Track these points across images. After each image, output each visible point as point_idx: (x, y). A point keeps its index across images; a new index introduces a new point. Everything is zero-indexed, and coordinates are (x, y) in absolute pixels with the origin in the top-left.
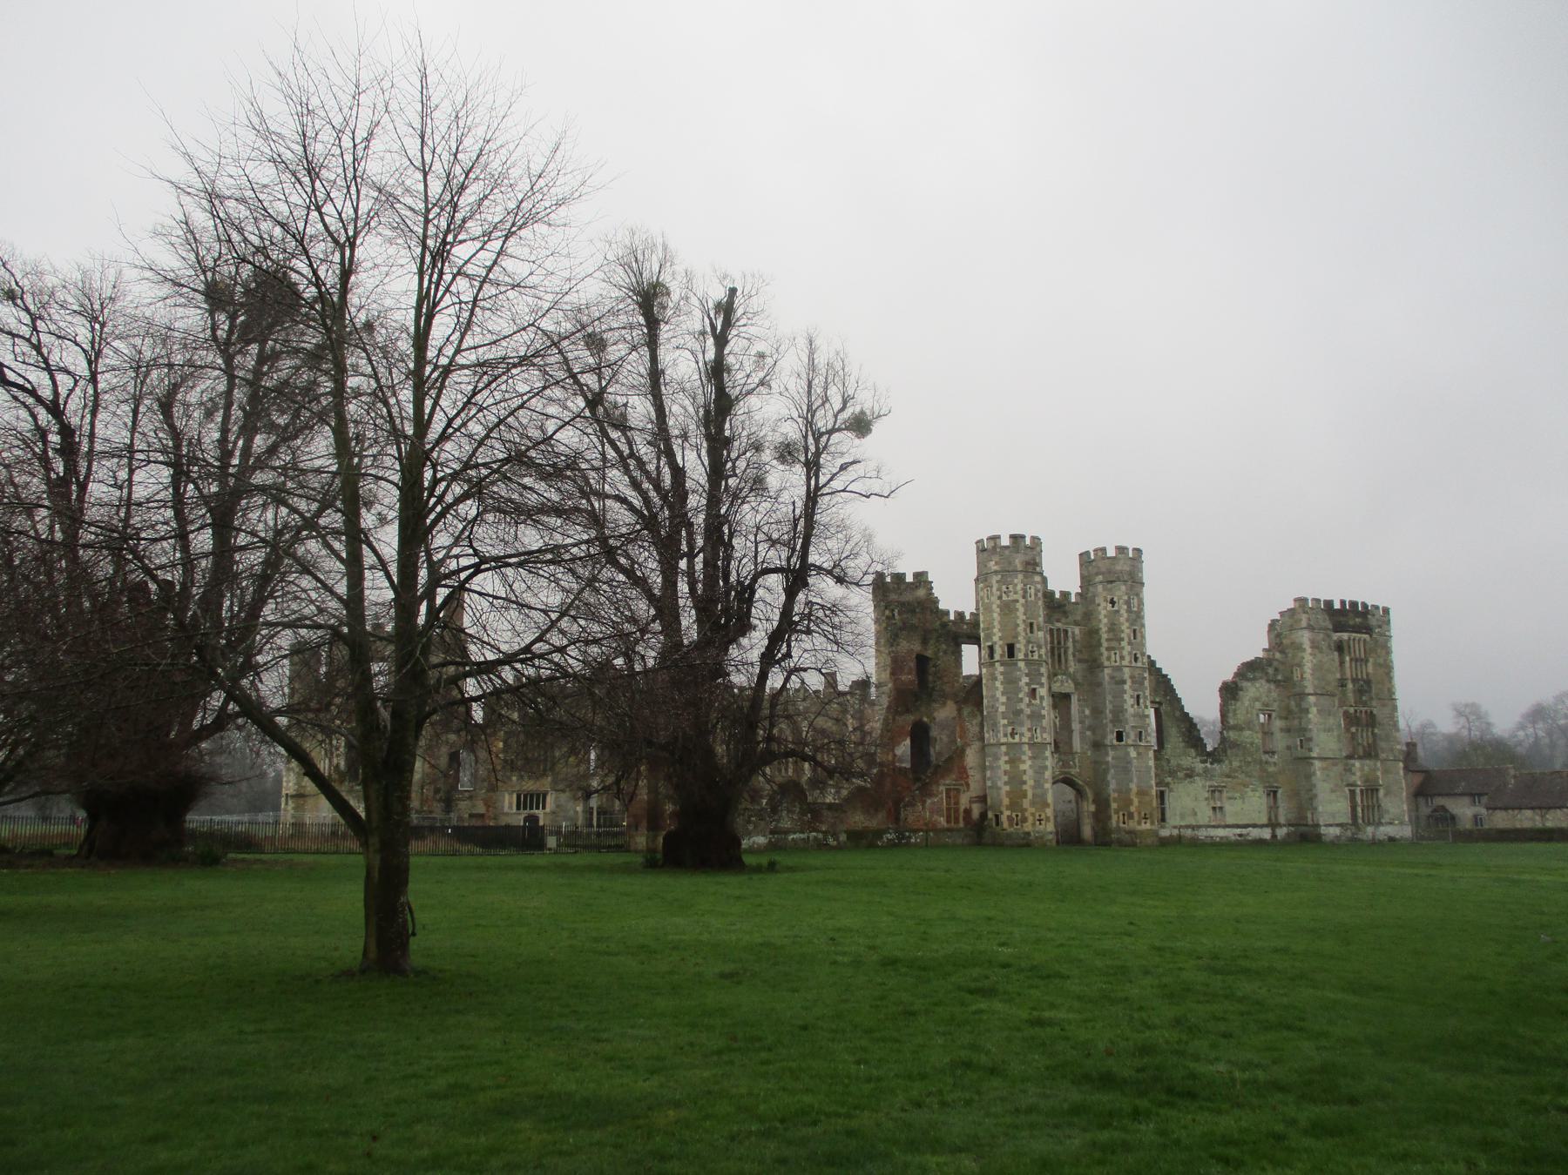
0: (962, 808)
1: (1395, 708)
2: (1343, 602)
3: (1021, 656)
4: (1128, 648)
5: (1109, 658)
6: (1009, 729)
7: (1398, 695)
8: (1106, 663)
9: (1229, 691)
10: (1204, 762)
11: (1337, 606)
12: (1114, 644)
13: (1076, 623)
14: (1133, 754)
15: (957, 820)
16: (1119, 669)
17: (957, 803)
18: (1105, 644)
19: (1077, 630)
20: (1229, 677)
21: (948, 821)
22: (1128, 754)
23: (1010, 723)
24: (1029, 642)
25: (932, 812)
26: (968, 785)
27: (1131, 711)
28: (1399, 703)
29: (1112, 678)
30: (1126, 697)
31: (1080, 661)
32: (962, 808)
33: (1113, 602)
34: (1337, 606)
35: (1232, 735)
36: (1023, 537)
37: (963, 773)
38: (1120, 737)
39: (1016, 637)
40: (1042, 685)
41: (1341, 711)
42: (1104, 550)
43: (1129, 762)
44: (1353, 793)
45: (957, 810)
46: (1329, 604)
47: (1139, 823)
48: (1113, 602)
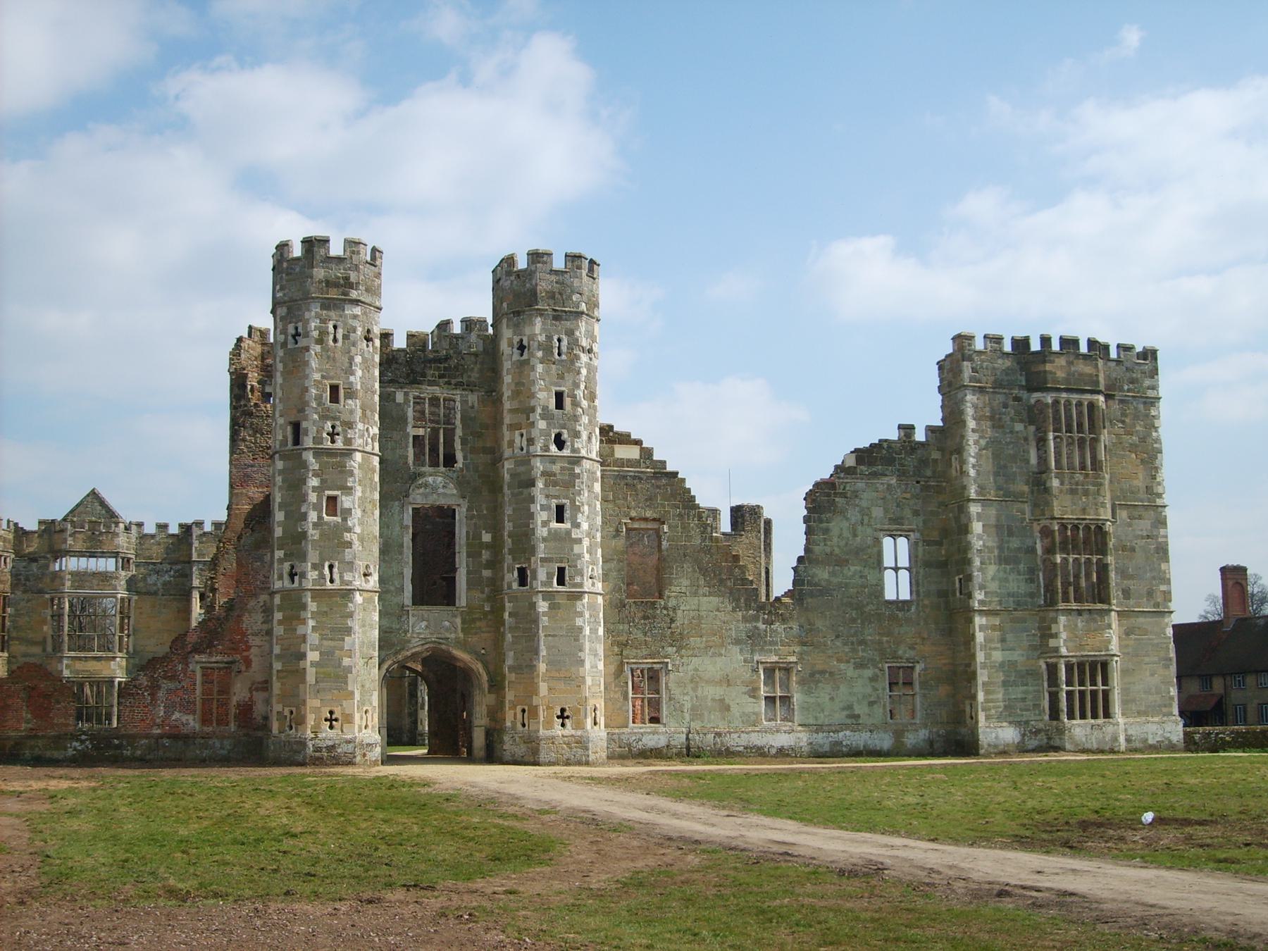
0: (234, 700)
1: (1162, 522)
2: (1045, 341)
3: (308, 442)
4: (542, 424)
5: (511, 443)
6: (287, 566)
7: (1166, 499)
8: (507, 453)
9: (823, 501)
10: (745, 619)
11: (1035, 346)
12: (521, 418)
13: (469, 387)
14: (543, 606)
15: (222, 721)
16: (526, 461)
17: (225, 690)
18: (507, 420)
19: (473, 398)
20: (826, 473)
21: (205, 721)
22: (533, 606)
23: (288, 556)
24: (324, 418)
25: (170, 709)
26: (248, 662)
27: (542, 532)
28: (1168, 512)
29: (513, 475)
30: (536, 508)
31: (474, 450)
32: (234, 700)
33: (522, 348)
34: (1035, 346)
35: (822, 574)
36: (325, 242)
37: (239, 645)
38: (523, 580)
39: (302, 410)
40: (348, 490)
41: (1036, 528)
42: (509, 261)
43: (536, 621)
44: (1052, 670)
45: (224, 704)
46: (1021, 344)
47: (549, 725)
48: (522, 348)
